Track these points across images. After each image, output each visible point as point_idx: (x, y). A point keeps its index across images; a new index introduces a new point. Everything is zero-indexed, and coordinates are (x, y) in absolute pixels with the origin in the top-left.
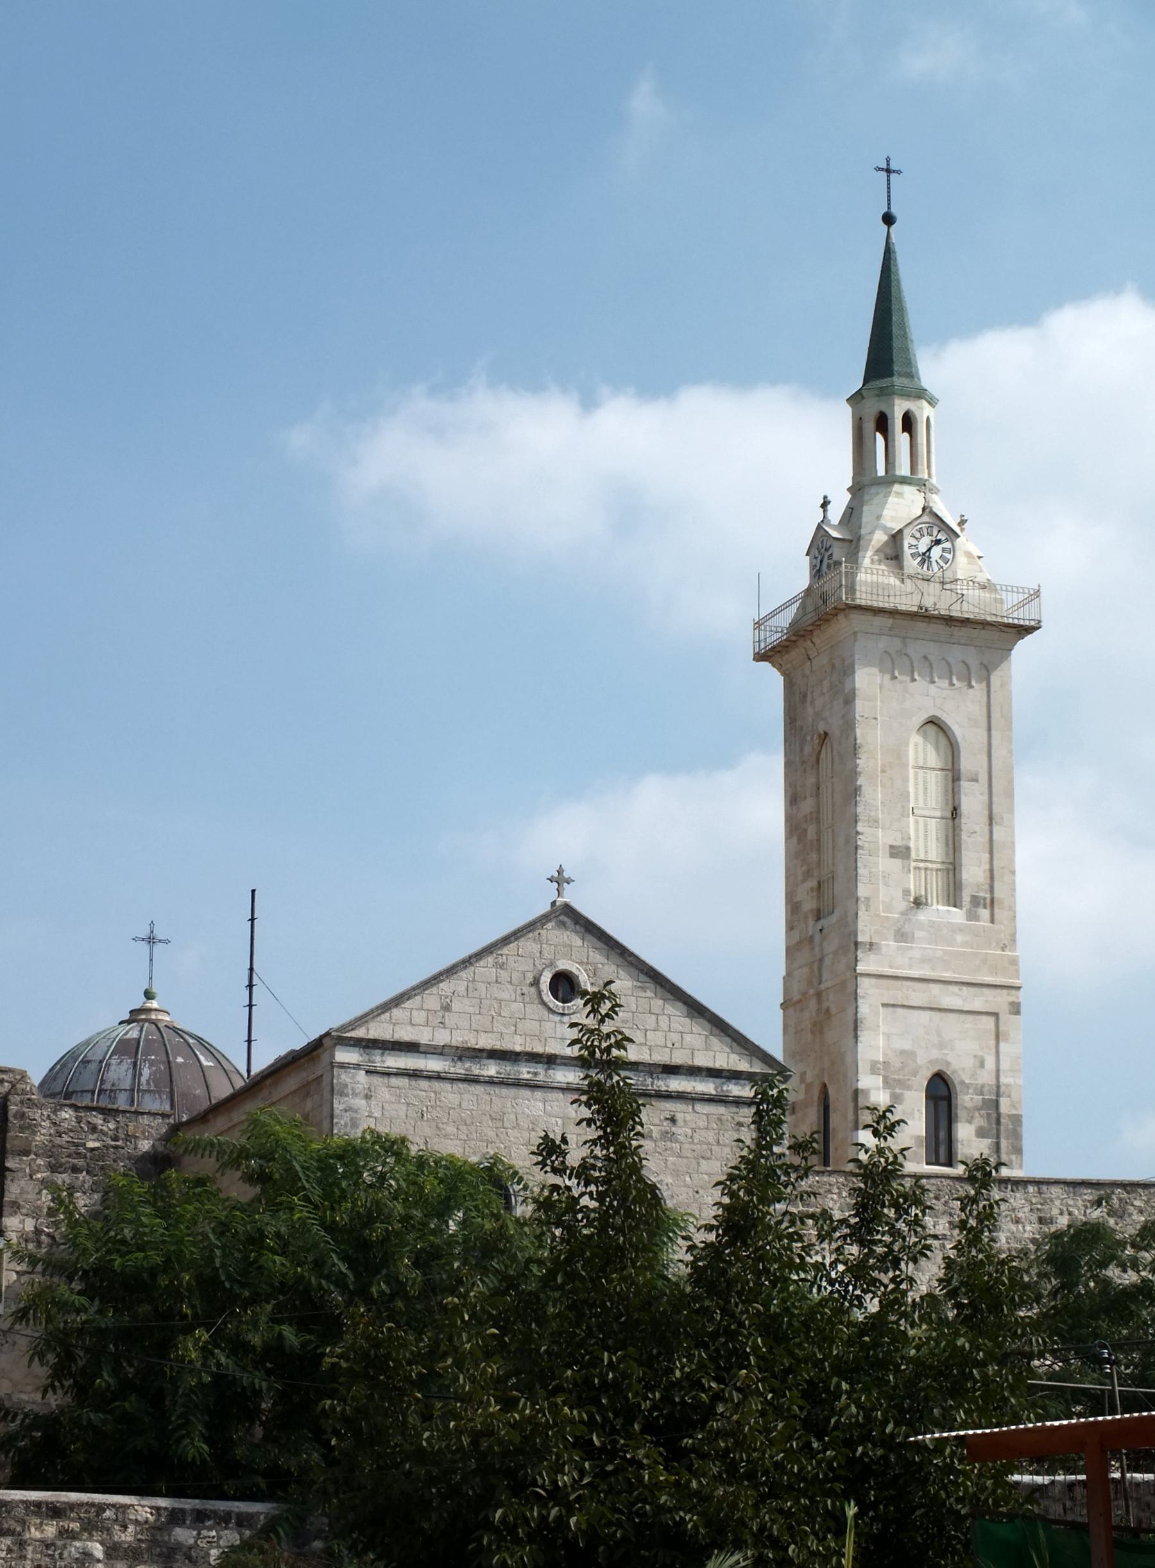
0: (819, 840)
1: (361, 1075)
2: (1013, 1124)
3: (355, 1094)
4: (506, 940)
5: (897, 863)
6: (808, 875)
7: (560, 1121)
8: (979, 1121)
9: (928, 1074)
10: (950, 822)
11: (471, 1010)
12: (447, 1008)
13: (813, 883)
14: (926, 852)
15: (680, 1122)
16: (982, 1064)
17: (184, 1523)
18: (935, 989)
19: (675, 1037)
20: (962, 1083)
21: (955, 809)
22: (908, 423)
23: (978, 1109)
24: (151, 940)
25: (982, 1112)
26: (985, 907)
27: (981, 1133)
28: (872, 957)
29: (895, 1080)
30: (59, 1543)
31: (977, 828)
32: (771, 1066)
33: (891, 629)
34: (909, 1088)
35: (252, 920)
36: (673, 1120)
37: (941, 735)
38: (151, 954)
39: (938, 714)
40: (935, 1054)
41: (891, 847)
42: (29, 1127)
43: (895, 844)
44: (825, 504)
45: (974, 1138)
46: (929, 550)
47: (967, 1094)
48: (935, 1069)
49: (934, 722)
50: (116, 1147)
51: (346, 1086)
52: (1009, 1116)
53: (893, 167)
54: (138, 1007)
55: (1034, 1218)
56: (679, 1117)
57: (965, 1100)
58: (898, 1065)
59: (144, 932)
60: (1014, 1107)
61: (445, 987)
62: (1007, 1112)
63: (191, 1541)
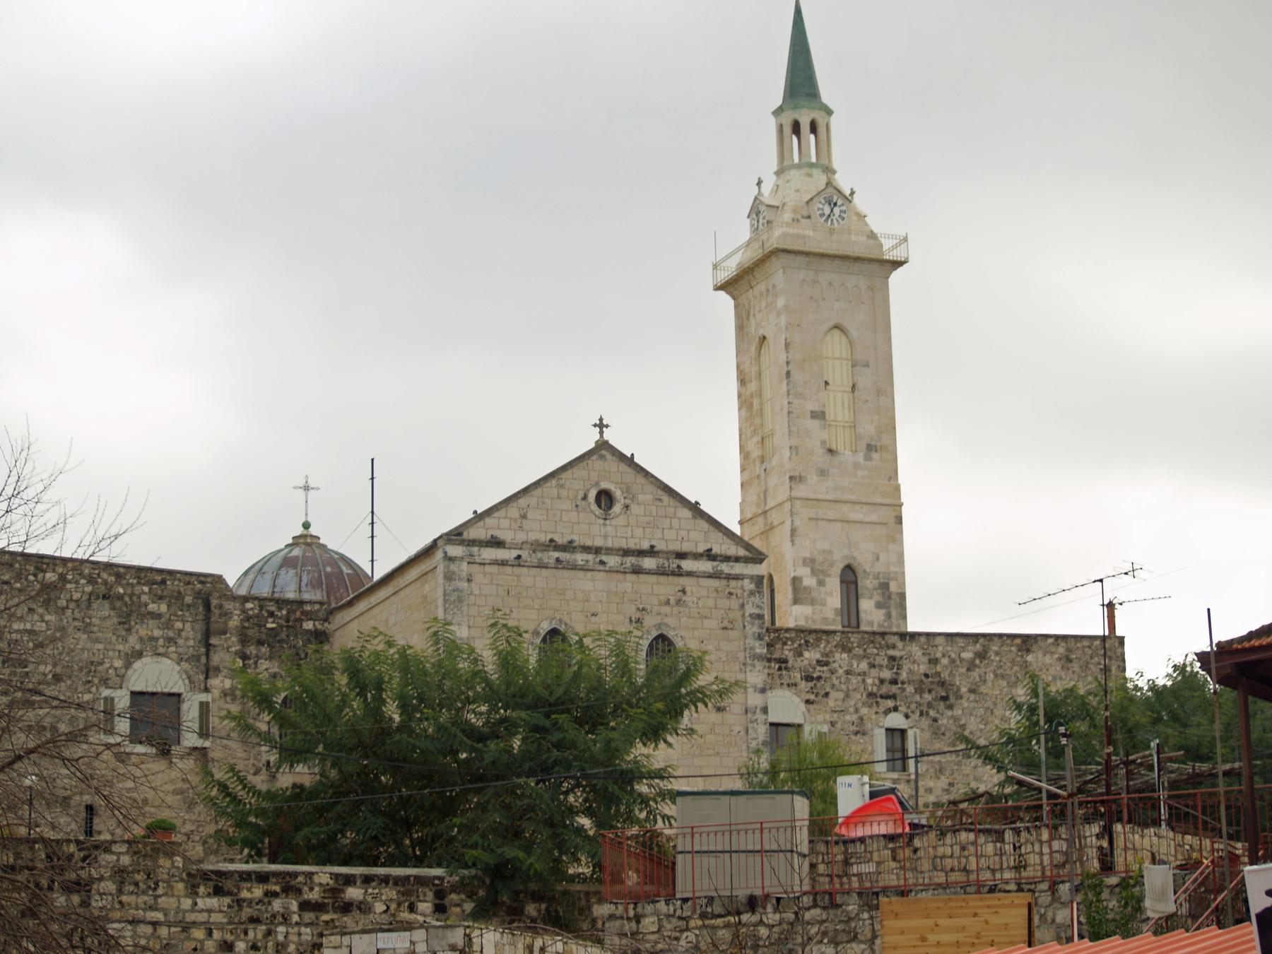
0: (761, 409)
1: (464, 565)
3: (460, 579)
4: (564, 469)
5: (816, 423)
6: (755, 432)
7: (605, 594)
8: (877, 597)
9: (842, 566)
10: (851, 395)
11: (541, 518)
12: (524, 517)
13: (757, 439)
14: (835, 415)
15: (689, 593)
16: (878, 559)
17: (355, 884)
18: (845, 508)
19: (684, 533)
21: (854, 386)
22: (814, 128)
23: (876, 589)
24: (306, 488)
27: (879, 606)
28: (801, 487)
30: (266, 900)
32: (751, 552)
34: (829, 575)
35: (372, 478)
36: (684, 591)
37: (843, 336)
38: (307, 496)
39: (841, 322)
40: (846, 552)
41: (812, 412)
42: (226, 614)
44: (759, 183)
45: (873, 609)
46: (832, 211)
48: (846, 563)
50: (287, 627)
51: (454, 573)
54: (298, 534)
55: (925, 659)
56: (688, 589)
57: (866, 583)
59: (302, 483)
61: (523, 502)
63: (361, 898)
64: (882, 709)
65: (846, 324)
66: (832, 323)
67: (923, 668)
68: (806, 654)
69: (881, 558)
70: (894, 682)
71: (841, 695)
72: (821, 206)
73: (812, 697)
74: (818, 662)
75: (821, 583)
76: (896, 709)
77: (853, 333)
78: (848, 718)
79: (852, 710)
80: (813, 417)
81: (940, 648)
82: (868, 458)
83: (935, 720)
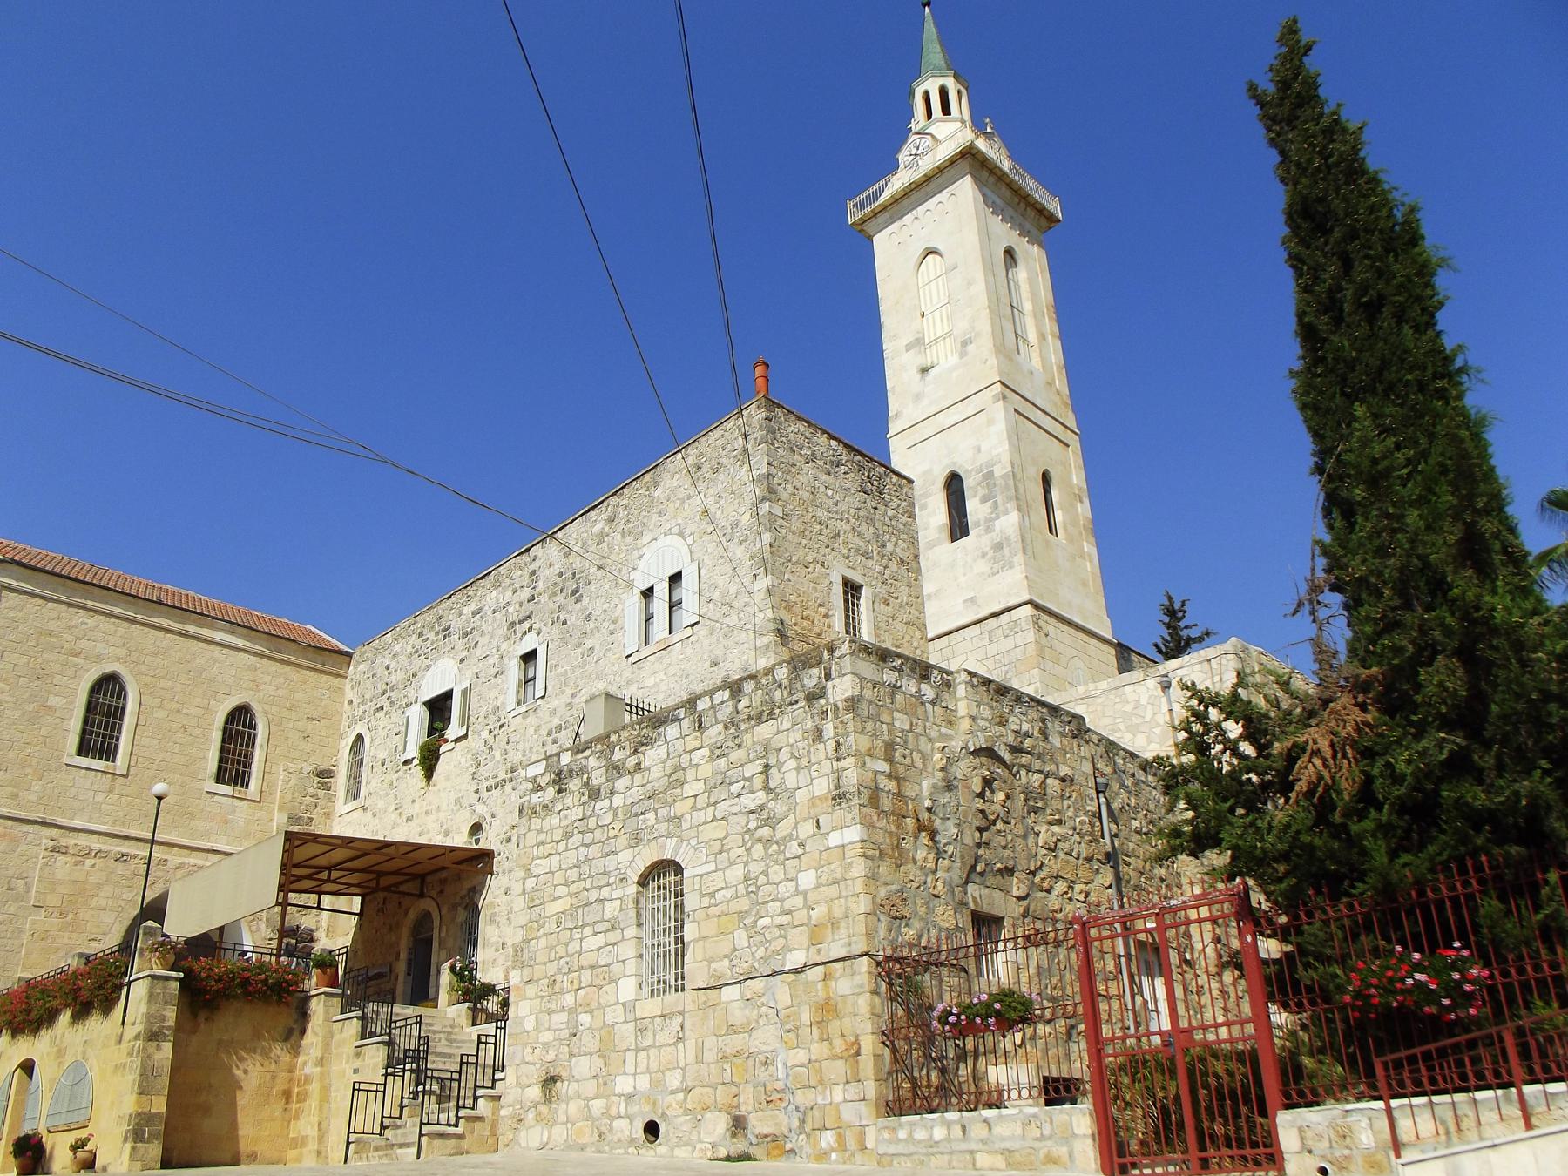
16: (979, 450)
20: (967, 471)
23: (979, 484)
48: (946, 472)
57: (969, 483)
60: (1005, 468)
64: (519, 635)
67: (557, 569)
68: (466, 610)
69: (983, 449)
70: (532, 599)
71: (488, 637)
73: (465, 653)
74: (474, 614)
76: (530, 630)
78: (491, 661)
79: (495, 650)
81: (574, 536)
82: (963, 354)
83: (564, 623)
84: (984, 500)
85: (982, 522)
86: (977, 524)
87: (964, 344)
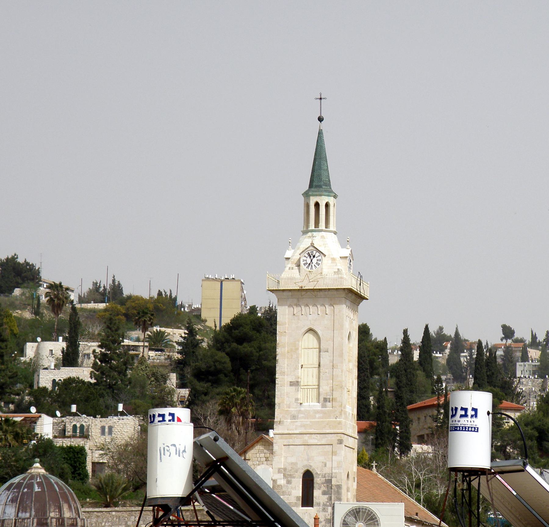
2: (337, 489)
8: (323, 488)
16: (325, 465)
18: (306, 437)
20: (317, 473)
23: (323, 483)
25: (324, 485)
26: (329, 402)
27: (324, 493)
28: (280, 426)
29: (288, 475)
31: (327, 371)
33: (292, 296)
34: (294, 477)
40: (305, 463)
41: (291, 382)
43: (292, 381)
45: (321, 495)
47: (319, 478)
49: (311, 330)
52: (335, 485)
53: (322, 100)
57: (318, 480)
58: (290, 469)
60: (338, 482)
62: (335, 484)
65: (314, 328)
66: (306, 328)
72: (305, 259)
75: (289, 482)
77: (319, 332)
80: (291, 385)
84: (324, 493)
85: (321, 505)
86: (319, 504)
87: (325, 400)
